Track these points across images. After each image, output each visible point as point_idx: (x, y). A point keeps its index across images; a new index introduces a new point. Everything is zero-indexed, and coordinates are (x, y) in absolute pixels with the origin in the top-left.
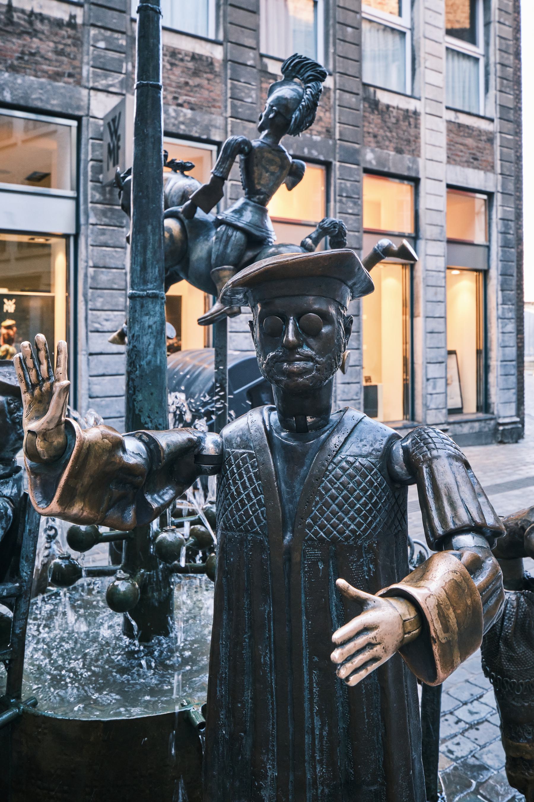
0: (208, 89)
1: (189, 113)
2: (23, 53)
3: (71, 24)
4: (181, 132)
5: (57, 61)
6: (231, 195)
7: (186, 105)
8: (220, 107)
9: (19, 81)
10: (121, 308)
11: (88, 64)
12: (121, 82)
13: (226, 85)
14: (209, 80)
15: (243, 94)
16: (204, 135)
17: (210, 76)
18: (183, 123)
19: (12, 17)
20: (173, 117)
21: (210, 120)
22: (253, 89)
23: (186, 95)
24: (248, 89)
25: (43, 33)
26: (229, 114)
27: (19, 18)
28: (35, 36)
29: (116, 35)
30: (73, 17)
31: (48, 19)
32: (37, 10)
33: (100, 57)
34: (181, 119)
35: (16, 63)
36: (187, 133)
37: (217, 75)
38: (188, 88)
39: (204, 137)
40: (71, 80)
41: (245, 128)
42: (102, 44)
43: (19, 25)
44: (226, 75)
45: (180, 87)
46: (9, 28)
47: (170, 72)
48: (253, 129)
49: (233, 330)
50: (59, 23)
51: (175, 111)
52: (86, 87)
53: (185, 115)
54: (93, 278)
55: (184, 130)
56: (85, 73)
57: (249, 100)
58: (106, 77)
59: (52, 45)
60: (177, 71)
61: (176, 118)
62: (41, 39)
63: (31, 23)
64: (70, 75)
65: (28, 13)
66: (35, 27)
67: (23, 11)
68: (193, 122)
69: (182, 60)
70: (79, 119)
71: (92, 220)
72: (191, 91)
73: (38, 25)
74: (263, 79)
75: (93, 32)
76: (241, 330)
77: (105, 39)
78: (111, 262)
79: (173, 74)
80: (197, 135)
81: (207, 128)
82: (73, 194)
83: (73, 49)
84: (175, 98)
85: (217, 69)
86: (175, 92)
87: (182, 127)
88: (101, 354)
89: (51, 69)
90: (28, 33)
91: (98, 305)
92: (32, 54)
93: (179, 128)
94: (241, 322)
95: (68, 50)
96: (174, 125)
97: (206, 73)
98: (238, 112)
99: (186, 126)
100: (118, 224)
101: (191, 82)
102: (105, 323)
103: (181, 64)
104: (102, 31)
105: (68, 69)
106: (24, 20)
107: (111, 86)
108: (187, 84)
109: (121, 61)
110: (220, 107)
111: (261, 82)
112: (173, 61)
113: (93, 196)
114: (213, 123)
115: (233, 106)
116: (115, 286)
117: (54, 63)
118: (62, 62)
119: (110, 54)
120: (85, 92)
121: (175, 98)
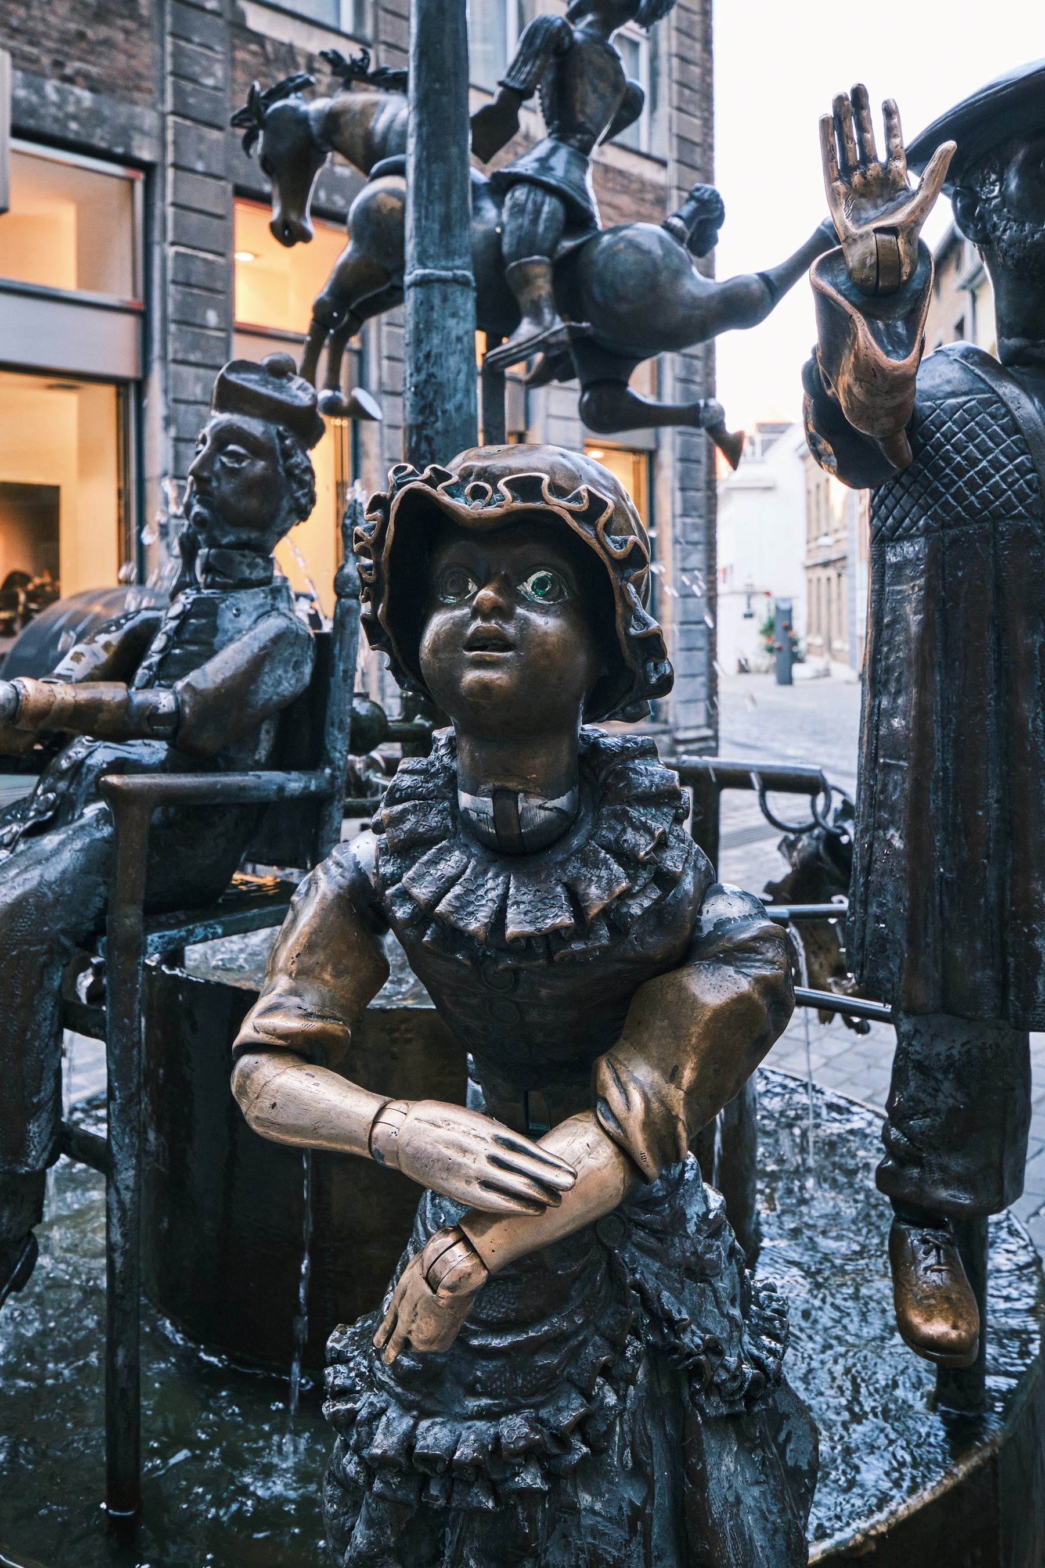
0: (126, 52)
4: (71, 136)
6: (175, 273)
7: (80, 80)
8: (150, 91)
13: (163, 46)
14: (127, 32)
15: (197, 69)
16: (117, 145)
18: (74, 117)
20: (54, 104)
21: (131, 117)
22: (218, 61)
24: (208, 58)
26: (169, 106)
34: (71, 109)
36: (83, 138)
37: (143, 24)
39: (119, 150)
41: (201, 139)
44: (163, 25)
48: (217, 142)
51: (58, 90)
53: (78, 101)
55: (77, 133)
57: (210, 82)
61: (59, 106)
68: (95, 117)
72: (92, 52)
74: (237, 42)
79: (54, 13)
80: (103, 145)
81: (126, 132)
84: (58, 64)
85: (144, 12)
86: (58, 51)
87: (73, 126)
93: (66, 127)
96: (56, 120)
97: (122, 17)
98: (186, 105)
101: (90, 34)
108: (81, 36)
110: (150, 91)
111: (234, 48)
114: (137, 122)
115: (178, 93)
121: (58, 64)
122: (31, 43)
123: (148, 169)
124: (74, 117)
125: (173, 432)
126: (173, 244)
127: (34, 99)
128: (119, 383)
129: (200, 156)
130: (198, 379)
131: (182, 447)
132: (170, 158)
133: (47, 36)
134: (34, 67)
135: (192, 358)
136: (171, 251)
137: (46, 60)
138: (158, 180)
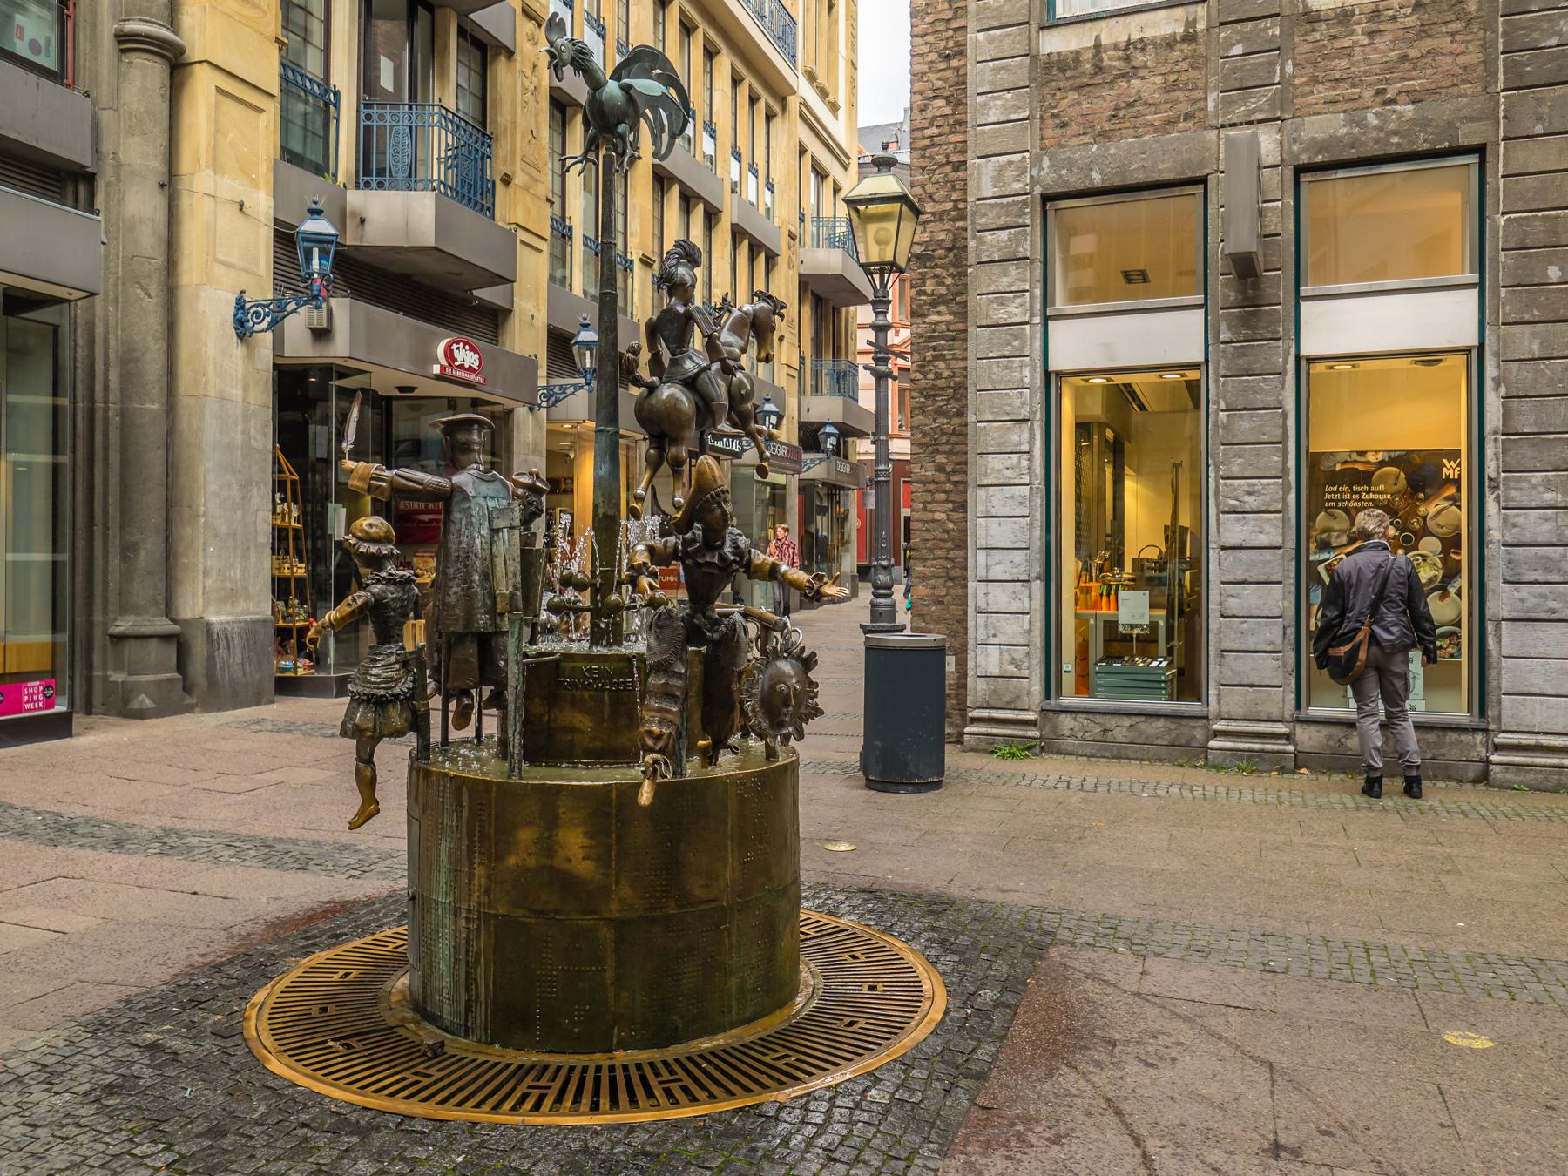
1: (1408, 110)
2: (1117, 108)
3: (1189, 38)
4: (1392, 150)
5: (1166, 102)
7: (1403, 97)
9: (1112, 151)
10: (1274, 473)
11: (1215, 88)
12: (1273, 99)
15: (1536, 35)
17: (1459, 26)
18: (1396, 133)
19: (1101, 60)
20: (1375, 128)
23: (1403, 79)
24: (1550, 19)
25: (1145, 67)
26: (1501, 86)
27: (1110, 59)
28: (1135, 76)
29: (1262, 24)
30: (1191, 23)
31: (1153, 43)
32: (1135, 37)
33: (1234, 70)
34: (1392, 126)
35: (1107, 126)
36: (1407, 149)
38: (1407, 65)
40: (1189, 124)
42: (1238, 49)
43: (1111, 68)
45: (1390, 70)
46: (1097, 80)
47: (1368, 49)
49: (1512, 504)
50: (1169, 43)
51: (1377, 114)
52: (1213, 128)
53: (1400, 115)
54: (1225, 428)
56: (1211, 105)
57: (1554, 41)
58: (1245, 100)
59: (1158, 79)
60: (1382, 43)
61: (1379, 129)
62: (1143, 78)
63: (1127, 59)
64: (1187, 117)
65: (1123, 46)
66: (1134, 63)
67: (1116, 47)
68: (1421, 123)
69: (1394, 18)
70: (1203, 181)
71: (1222, 337)
72: (1414, 69)
73: (1139, 59)
75: (1224, 34)
76: (1534, 504)
77: (1244, 39)
78: (1259, 400)
80: (1427, 146)
82: (1199, 299)
83: (1193, 74)
87: (1395, 140)
88: (1241, 548)
89: (1155, 118)
90: (1124, 76)
91: (1235, 470)
92: (1130, 105)
93: (1388, 143)
94: (1534, 487)
95: (1184, 77)
96: (1377, 141)
98: (1521, 75)
99: (1402, 136)
100: (1269, 336)
101: (1413, 53)
102: (1246, 498)
103: (1390, 26)
104: (1238, 26)
105: (1184, 108)
106: (1119, 59)
107: (1254, 111)
109: (1272, 64)
112: (1374, 26)
113: (1225, 297)
116: (1265, 438)
117: (1163, 107)
118: (1176, 101)
119: (1252, 59)
120: (1212, 135)
122: (1353, 86)
123: (1480, 150)
124: (1396, 133)
125: (1503, 391)
126: (1504, 213)
127: (1356, 130)
128: (1467, 351)
129: (1539, 119)
130: (1534, 335)
131: (1514, 404)
132: (1501, 135)
133: (1367, 73)
134: (1355, 105)
135: (1527, 317)
136: (1502, 220)
137: (1368, 94)
138: (1489, 158)
